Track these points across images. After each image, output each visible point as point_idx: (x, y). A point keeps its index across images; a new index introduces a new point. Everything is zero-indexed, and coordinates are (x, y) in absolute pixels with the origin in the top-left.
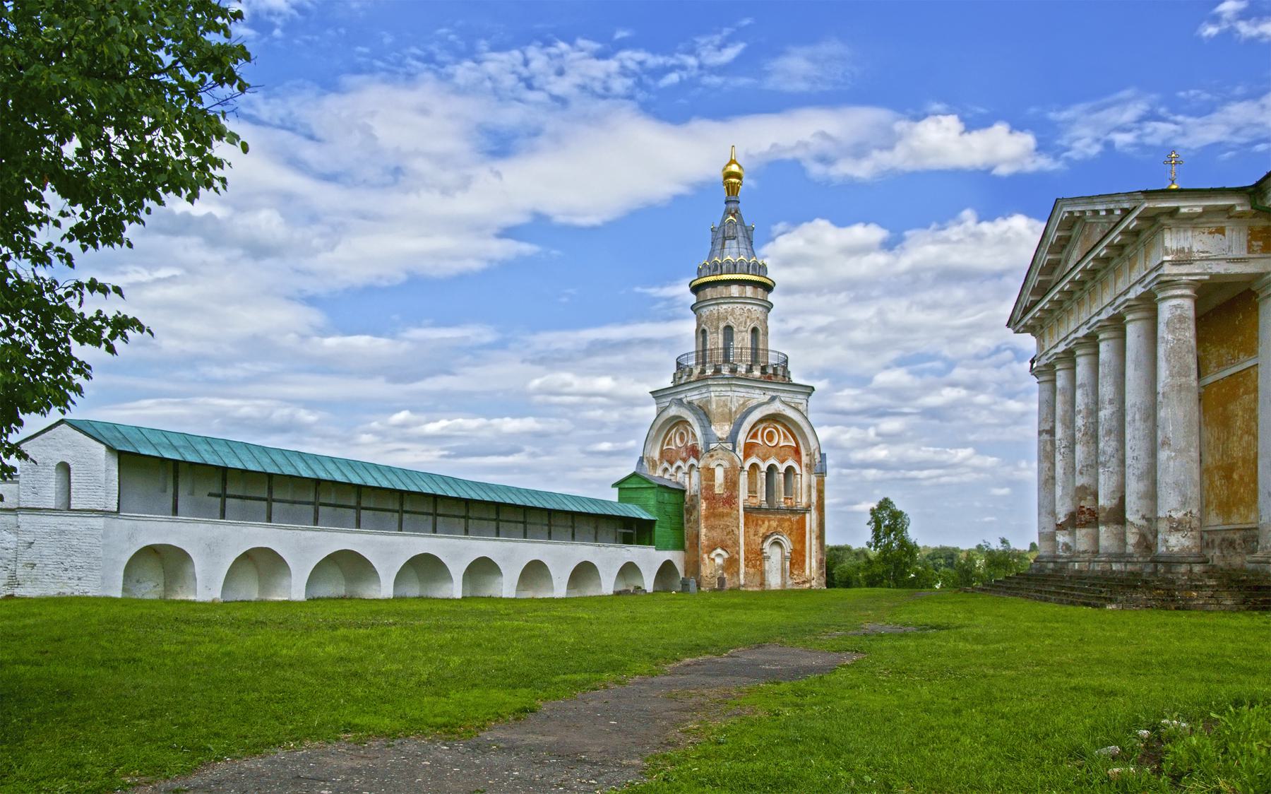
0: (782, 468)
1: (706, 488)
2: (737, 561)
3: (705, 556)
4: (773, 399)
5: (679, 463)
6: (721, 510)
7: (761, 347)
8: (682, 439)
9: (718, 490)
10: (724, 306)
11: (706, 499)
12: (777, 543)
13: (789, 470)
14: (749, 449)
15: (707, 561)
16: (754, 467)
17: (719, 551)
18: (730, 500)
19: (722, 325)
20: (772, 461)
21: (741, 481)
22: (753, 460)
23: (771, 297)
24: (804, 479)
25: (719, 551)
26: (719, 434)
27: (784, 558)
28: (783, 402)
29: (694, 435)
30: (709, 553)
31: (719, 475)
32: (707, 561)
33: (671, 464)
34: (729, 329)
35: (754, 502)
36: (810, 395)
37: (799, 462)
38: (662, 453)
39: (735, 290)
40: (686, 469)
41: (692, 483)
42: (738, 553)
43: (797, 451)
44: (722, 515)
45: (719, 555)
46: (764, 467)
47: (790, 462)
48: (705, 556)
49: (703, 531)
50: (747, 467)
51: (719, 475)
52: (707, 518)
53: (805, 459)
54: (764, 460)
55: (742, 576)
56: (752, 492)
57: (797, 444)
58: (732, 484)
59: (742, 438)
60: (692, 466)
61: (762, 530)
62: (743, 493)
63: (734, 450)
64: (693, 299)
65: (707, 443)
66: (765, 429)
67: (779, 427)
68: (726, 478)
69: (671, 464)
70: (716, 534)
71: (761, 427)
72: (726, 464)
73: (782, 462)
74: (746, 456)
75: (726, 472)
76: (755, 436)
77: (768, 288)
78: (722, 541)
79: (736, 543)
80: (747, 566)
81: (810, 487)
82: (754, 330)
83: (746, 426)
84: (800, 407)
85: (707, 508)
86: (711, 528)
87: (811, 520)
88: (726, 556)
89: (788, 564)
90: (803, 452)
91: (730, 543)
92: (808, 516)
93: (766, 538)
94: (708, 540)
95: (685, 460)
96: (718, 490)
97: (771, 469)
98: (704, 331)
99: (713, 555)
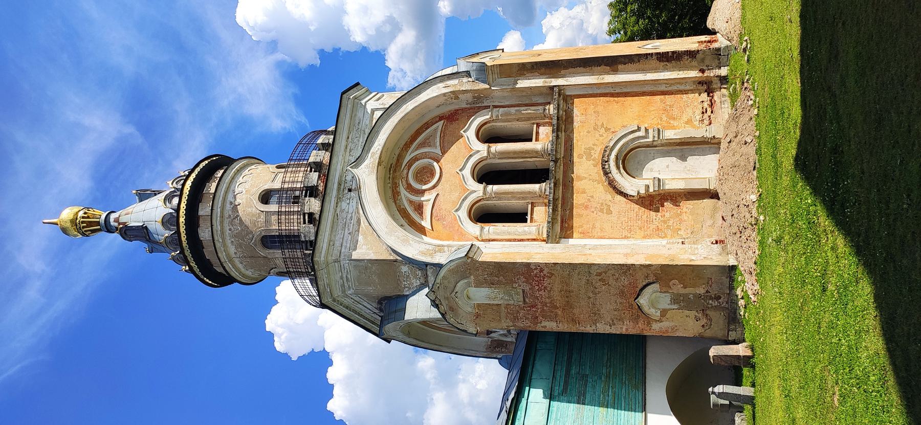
3: (656, 327)
6: (556, 295)
10: (232, 250)
15: (665, 324)
17: (643, 301)
19: (263, 252)
28: (358, 162)
30: (648, 320)
32: (665, 324)
35: (541, 214)
44: (567, 293)
45: (652, 305)
47: (471, 133)
49: (602, 328)
50: (474, 229)
57: (441, 118)
61: (601, 192)
63: (439, 266)
66: (410, 188)
68: (491, 284)
71: (403, 192)
75: (478, 285)
78: (622, 294)
84: (378, 114)
85: (554, 318)
86: (596, 316)
88: (656, 286)
91: (625, 281)
94: (621, 320)
99: (654, 313)
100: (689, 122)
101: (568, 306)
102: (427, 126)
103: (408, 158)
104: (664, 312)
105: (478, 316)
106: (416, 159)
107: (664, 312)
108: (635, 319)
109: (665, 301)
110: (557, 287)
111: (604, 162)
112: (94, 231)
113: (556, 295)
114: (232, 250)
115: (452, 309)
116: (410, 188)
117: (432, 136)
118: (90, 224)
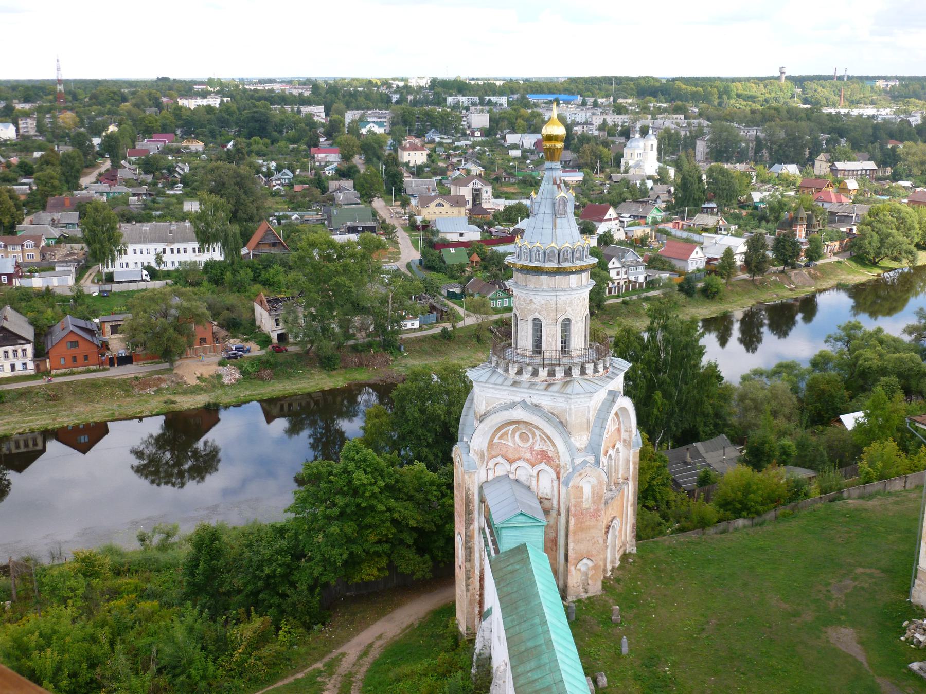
1: (575, 506)
6: (588, 523)
9: (585, 506)
11: (575, 515)
17: (585, 561)
25: (585, 561)
26: (578, 445)
38: (491, 444)
52: (575, 533)
70: (583, 547)
72: (594, 480)
75: (593, 487)
78: (588, 552)
81: (628, 461)
85: (576, 524)
86: (577, 542)
91: (594, 552)
96: (585, 506)
99: (578, 567)
101: (582, 529)
105: (577, 487)
108: (575, 559)
110: (592, 524)
113: (588, 523)
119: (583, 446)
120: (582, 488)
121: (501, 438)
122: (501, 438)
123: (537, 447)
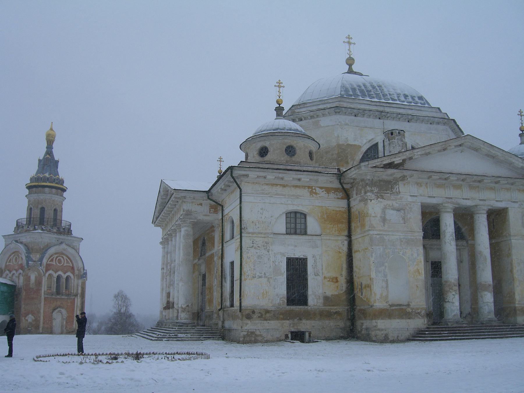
0: (65, 276)
2: (39, 321)
4: (61, 243)
5: (14, 272)
7: (58, 217)
8: (16, 260)
12: (60, 312)
13: (68, 278)
14: (48, 267)
15: (24, 321)
16: (50, 275)
17: (30, 315)
18: (38, 290)
19: (40, 206)
20: (60, 273)
21: (43, 282)
22: (51, 272)
23: (65, 194)
24: (75, 282)
25: (30, 315)
27: (63, 319)
29: (22, 258)
31: (33, 278)
32: (24, 321)
33: (10, 272)
34: (43, 210)
36: (81, 242)
37: (73, 273)
39: (47, 190)
40: (17, 275)
41: (20, 282)
42: (40, 317)
43: (73, 268)
46: (55, 275)
47: (69, 274)
48: (23, 318)
49: (23, 306)
50: (47, 274)
51: (33, 278)
53: (76, 272)
54: (56, 272)
55: (41, 329)
56: (49, 287)
58: (39, 283)
59: (45, 261)
60: (20, 274)
62: (44, 288)
64: (27, 192)
65: (28, 263)
67: (65, 257)
68: (36, 281)
69: (10, 272)
71: (56, 256)
73: (65, 273)
74: (47, 270)
75: (36, 277)
76: (52, 260)
77: (64, 190)
79: (39, 312)
80: (44, 323)
82: (55, 210)
83: (47, 256)
87: (78, 301)
89: (65, 323)
90: (76, 269)
92: (76, 299)
93: (54, 309)
95: (17, 271)
97: (59, 278)
98: (31, 209)
99: (27, 318)
100: (66, 327)
102: (71, 261)
103: (65, 257)
104: (27, 320)
106: (63, 258)
107: (27, 320)
109: (30, 320)
111: (60, 307)
112: (48, 142)
114: (42, 197)
115: (29, 269)
116: (57, 257)
117: (69, 263)
118: (50, 142)
119: (37, 260)
120: (30, 277)
121: (9, 262)
122: (9, 262)
123: (20, 263)
